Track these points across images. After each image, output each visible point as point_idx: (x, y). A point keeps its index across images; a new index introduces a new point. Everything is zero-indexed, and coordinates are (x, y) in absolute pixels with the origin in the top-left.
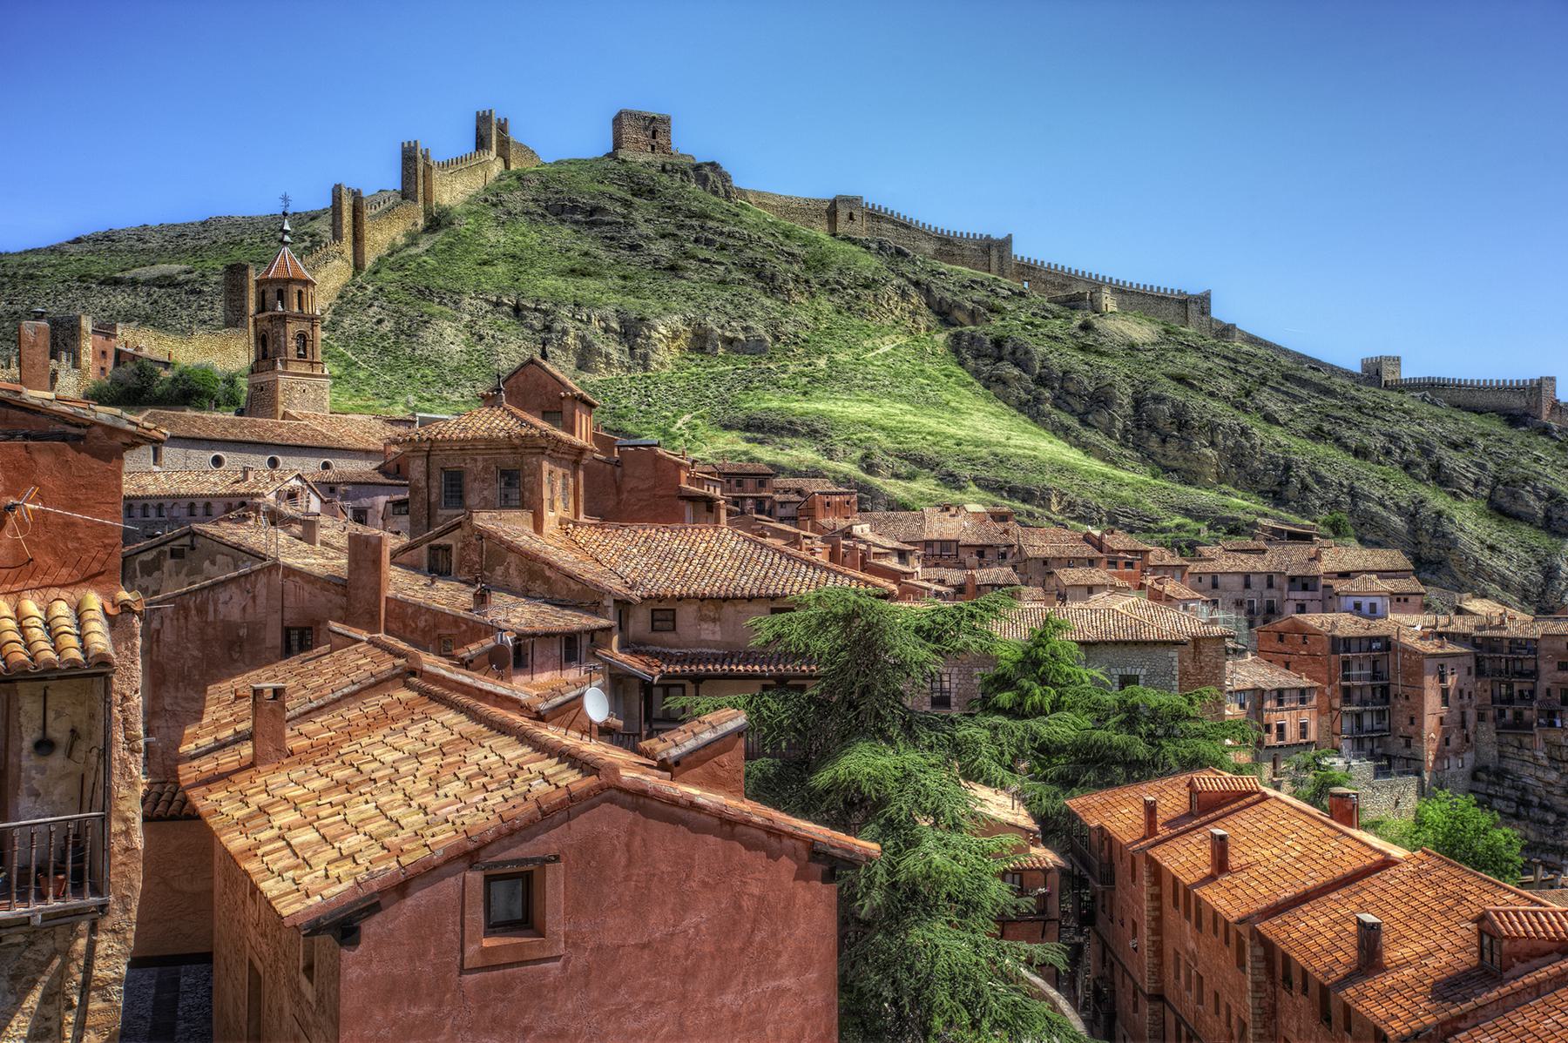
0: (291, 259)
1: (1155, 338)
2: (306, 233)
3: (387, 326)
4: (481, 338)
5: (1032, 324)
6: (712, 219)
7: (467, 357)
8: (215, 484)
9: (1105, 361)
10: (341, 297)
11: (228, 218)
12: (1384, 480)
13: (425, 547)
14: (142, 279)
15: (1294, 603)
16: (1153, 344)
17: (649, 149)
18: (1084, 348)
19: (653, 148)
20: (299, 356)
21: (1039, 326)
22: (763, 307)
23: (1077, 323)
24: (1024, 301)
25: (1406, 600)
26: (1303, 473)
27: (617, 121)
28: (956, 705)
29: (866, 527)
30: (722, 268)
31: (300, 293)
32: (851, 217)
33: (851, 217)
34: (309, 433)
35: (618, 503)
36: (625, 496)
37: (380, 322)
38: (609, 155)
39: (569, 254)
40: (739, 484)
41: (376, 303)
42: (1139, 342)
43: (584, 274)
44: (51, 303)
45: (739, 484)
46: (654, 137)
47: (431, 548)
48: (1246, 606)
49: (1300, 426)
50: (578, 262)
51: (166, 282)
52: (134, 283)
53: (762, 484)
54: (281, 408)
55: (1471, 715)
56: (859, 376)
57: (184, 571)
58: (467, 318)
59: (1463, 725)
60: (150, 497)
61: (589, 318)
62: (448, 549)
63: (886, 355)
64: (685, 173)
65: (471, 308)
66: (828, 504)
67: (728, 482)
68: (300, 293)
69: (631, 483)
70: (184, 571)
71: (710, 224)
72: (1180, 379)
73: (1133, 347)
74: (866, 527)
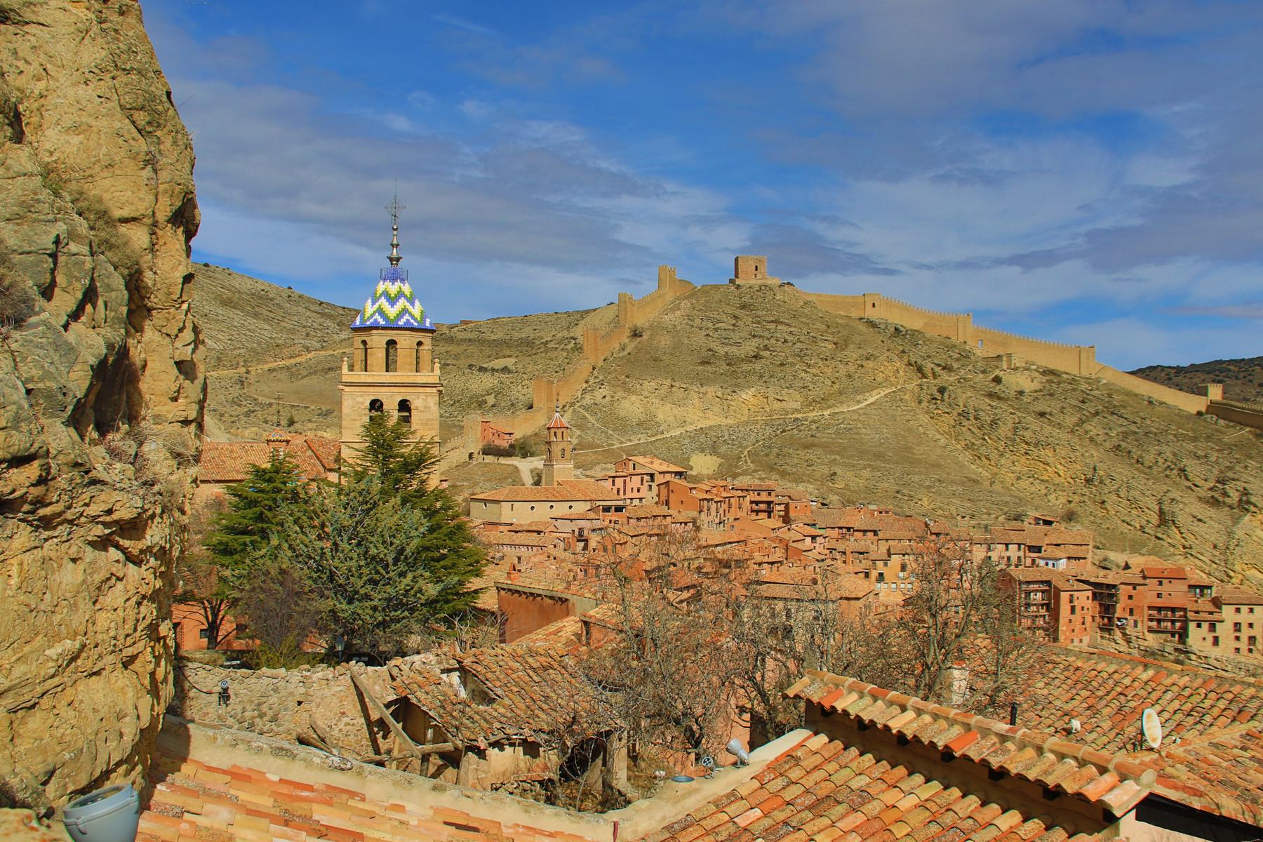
3: (608, 398)
6: (781, 323)
18: (991, 395)
26: (1102, 473)
37: (604, 397)
40: (759, 494)
45: (759, 494)
49: (1108, 445)
50: (704, 353)
51: (505, 370)
52: (493, 370)
53: (770, 494)
55: (1088, 619)
59: (1083, 623)
64: (771, 289)
71: (779, 327)
72: (1042, 414)
73: (1021, 393)
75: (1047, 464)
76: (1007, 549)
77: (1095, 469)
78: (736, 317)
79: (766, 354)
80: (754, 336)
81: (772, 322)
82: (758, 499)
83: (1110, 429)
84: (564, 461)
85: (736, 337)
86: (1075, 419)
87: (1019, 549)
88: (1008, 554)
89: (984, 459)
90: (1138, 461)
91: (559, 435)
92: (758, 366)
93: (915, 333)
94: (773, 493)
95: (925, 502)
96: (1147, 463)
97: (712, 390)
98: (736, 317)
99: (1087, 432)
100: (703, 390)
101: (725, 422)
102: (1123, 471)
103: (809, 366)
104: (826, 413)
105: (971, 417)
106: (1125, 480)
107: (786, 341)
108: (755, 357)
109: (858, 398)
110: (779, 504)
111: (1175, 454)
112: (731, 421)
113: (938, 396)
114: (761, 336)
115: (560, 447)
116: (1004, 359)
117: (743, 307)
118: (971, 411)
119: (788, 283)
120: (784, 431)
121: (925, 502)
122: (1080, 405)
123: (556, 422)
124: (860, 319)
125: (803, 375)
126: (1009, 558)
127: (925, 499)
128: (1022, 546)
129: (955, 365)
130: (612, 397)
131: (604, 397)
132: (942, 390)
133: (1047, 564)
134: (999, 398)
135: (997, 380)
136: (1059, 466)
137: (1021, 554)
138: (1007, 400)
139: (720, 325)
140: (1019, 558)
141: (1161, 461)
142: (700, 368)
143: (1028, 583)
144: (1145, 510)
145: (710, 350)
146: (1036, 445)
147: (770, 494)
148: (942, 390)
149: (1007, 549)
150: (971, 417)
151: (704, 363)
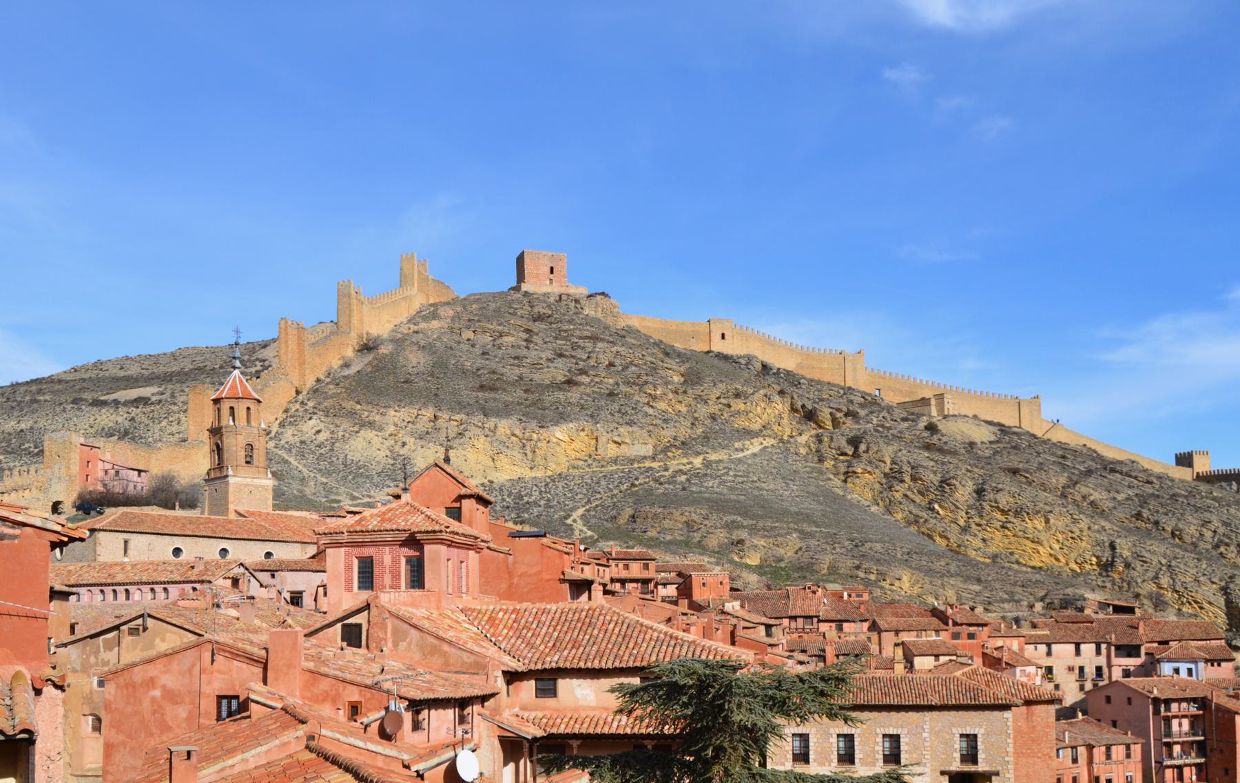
0: (241, 381)
1: (993, 438)
2: (257, 359)
3: (322, 437)
4: (404, 444)
5: (882, 426)
6: (602, 340)
7: (392, 462)
8: (171, 572)
9: (948, 458)
10: (286, 411)
11: (194, 348)
12: (1199, 560)
13: (339, 625)
14: (122, 400)
15: (1120, 669)
16: (991, 442)
17: (548, 282)
18: (928, 447)
19: (551, 280)
20: (247, 462)
21: (890, 428)
22: (646, 414)
23: (922, 423)
24: (875, 408)
25: (1219, 665)
26: (1126, 553)
27: (520, 260)
28: (815, 761)
29: (737, 604)
30: (611, 381)
31: (248, 409)
32: (723, 336)
33: (723, 336)
34: (254, 528)
35: (510, 586)
36: (515, 580)
37: (318, 432)
38: (513, 289)
39: (480, 373)
41: (315, 417)
42: (978, 441)
43: (493, 389)
44: (49, 421)
45: (626, 567)
46: (552, 272)
47: (344, 626)
48: (1077, 671)
50: (486, 378)
51: (144, 401)
52: (116, 403)
53: (646, 567)
54: (232, 507)
56: (731, 473)
57: (140, 647)
58: (392, 429)
60: (119, 584)
61: (496, 427)
62: (359, 626)
63: (754, 455)
65: (396, 419)
66: (704, 584)
67: (617, 565)
68: (248, 409)
69: (521, 569)
70: (140, 647)
71: (600, 345)
72: (1015, 472)
74: (737, 604)
75: (1039, 542)
76: (1078, 652)
77: (1113, 547)
78: (528, 331)
79: (585, 379)
80: (561, 355)
81: (587, 337)
82: (624, 574)
83: (1118, 492)
84: (250, 470)
85: (533, 355)
86: (1063, 480)
87: (1098, 652)
88: (1078, 662)
89: (938, 539)
90: (1173, 534)
91: (241, 413)
92: (574, 395)
93: (788, 373)
94: (652, 565)
95: (906, 583)
96: (1187, 539)
97: (505, 426)
98: (528, 331)
99: (1084, 497)
100: (491, 423)
101: (528, 474)
102: (1157, 551)
103: (654, 398)
104: (698, 461)
105: (907, 479)
106: (1164, 561)
107: (611, 365)
108: (570, 382)
109: (737, 445)
110: (665, 585)
111: (1225, 524)
112: (539, 474)
113: (850, 450)
114: (572, 356)
115: (242, 440)
116: (933, 402)
117: (539, 318)
118: (906, 468)
119: (603, 294)
120: (633, 485)
121: (906, 583)
122: (1060, 460)
123: (233, 387)
124: (708, 352)
125: (647, 409)
126: (1081, 669)
127: (905, 578)
128: (1104, 646)
129: (862, 413)
130: (332, 432)
131: (318, 432)
132: (855, 442)
133: (1177, 671)
134: (941, 450)
135: (931, 428)
136: (1056, 546)
137: (1102, 661)
138: (953, 453)
139: (505, 339)
140: (1099, 670)
141: (1208, 534)
142: (480, 394)
143: (1168, 702)
144: (1206, 605)
145: (494, 372)
146: (1017, 514)
147: (646, 567)
148: (855, 442)
149: (1078, 652)
150: (907, 479)
151: (482, 387)
